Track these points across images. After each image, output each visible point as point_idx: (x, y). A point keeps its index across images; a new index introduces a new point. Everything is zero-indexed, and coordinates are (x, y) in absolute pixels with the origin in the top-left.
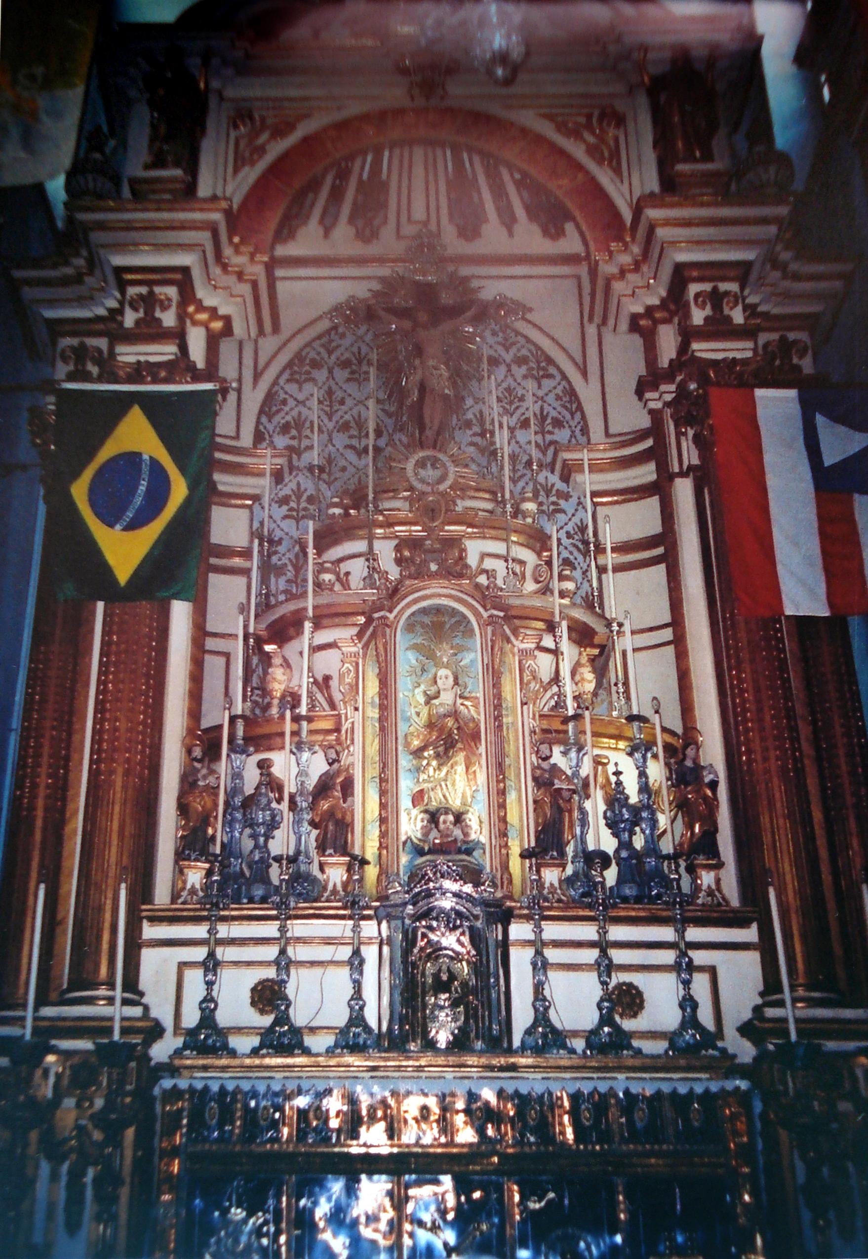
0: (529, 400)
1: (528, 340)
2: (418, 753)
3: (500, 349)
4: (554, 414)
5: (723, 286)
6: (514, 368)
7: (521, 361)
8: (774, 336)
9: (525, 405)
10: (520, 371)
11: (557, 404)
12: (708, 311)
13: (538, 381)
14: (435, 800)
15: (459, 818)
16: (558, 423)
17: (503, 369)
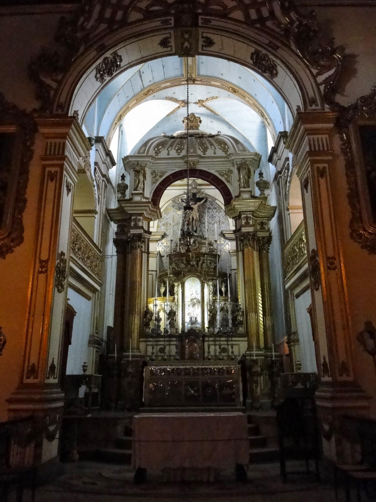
0: (217, 217)
1: (217, 204)
2: (189, 306)
3: (211, 206)
4: (222, 221)
5: (249, 215)
6: (214, 210)
7: (215, 208)
8: (261, 221)
9: (216, 218)
10: (215, 211)
11: (223, 218)
12: (245, 221)
13: (219, 213)
14: (192, 315)
15: (196, 318)
16: (223, 223)
17: (211, 210)
